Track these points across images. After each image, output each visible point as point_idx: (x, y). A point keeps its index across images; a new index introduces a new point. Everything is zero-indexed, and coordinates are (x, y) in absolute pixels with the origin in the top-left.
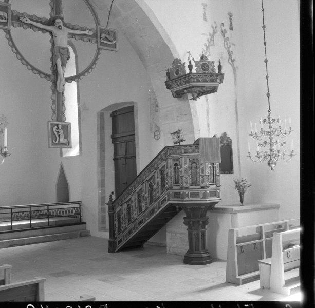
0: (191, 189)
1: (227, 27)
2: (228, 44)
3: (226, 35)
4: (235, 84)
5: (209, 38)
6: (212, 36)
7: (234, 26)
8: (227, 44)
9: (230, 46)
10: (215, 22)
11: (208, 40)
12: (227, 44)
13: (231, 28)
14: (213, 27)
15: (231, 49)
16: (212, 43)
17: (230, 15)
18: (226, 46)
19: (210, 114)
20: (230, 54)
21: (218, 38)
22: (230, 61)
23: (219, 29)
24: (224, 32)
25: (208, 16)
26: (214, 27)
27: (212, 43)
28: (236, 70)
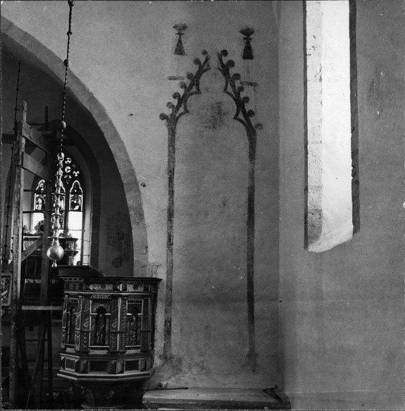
0: (68, 353)
1: (236, 54)
2: (238, 84)
3: (232, 71)
4: (252, 156)
5: (187, 82)
6: (195, 79)
7: (256, 52)
8: (233, 86)
9: (241, 89)
10: (205, 53)
11: (183, 86)
12: (233, 86)
13: (248, 54)
14: (197, 61)
15: (243, 95)
16: (194, 89)
17: (247, 33)
18: (230, 89)
19: (175, 220)
20: (241, 103)
21: (213, 82)
22: (241, 116)
23: (214, 62)
24: (225, 68)
25: (187, 46)
26: (202, 59)
27: (194, 89)
28: (254, 132)
